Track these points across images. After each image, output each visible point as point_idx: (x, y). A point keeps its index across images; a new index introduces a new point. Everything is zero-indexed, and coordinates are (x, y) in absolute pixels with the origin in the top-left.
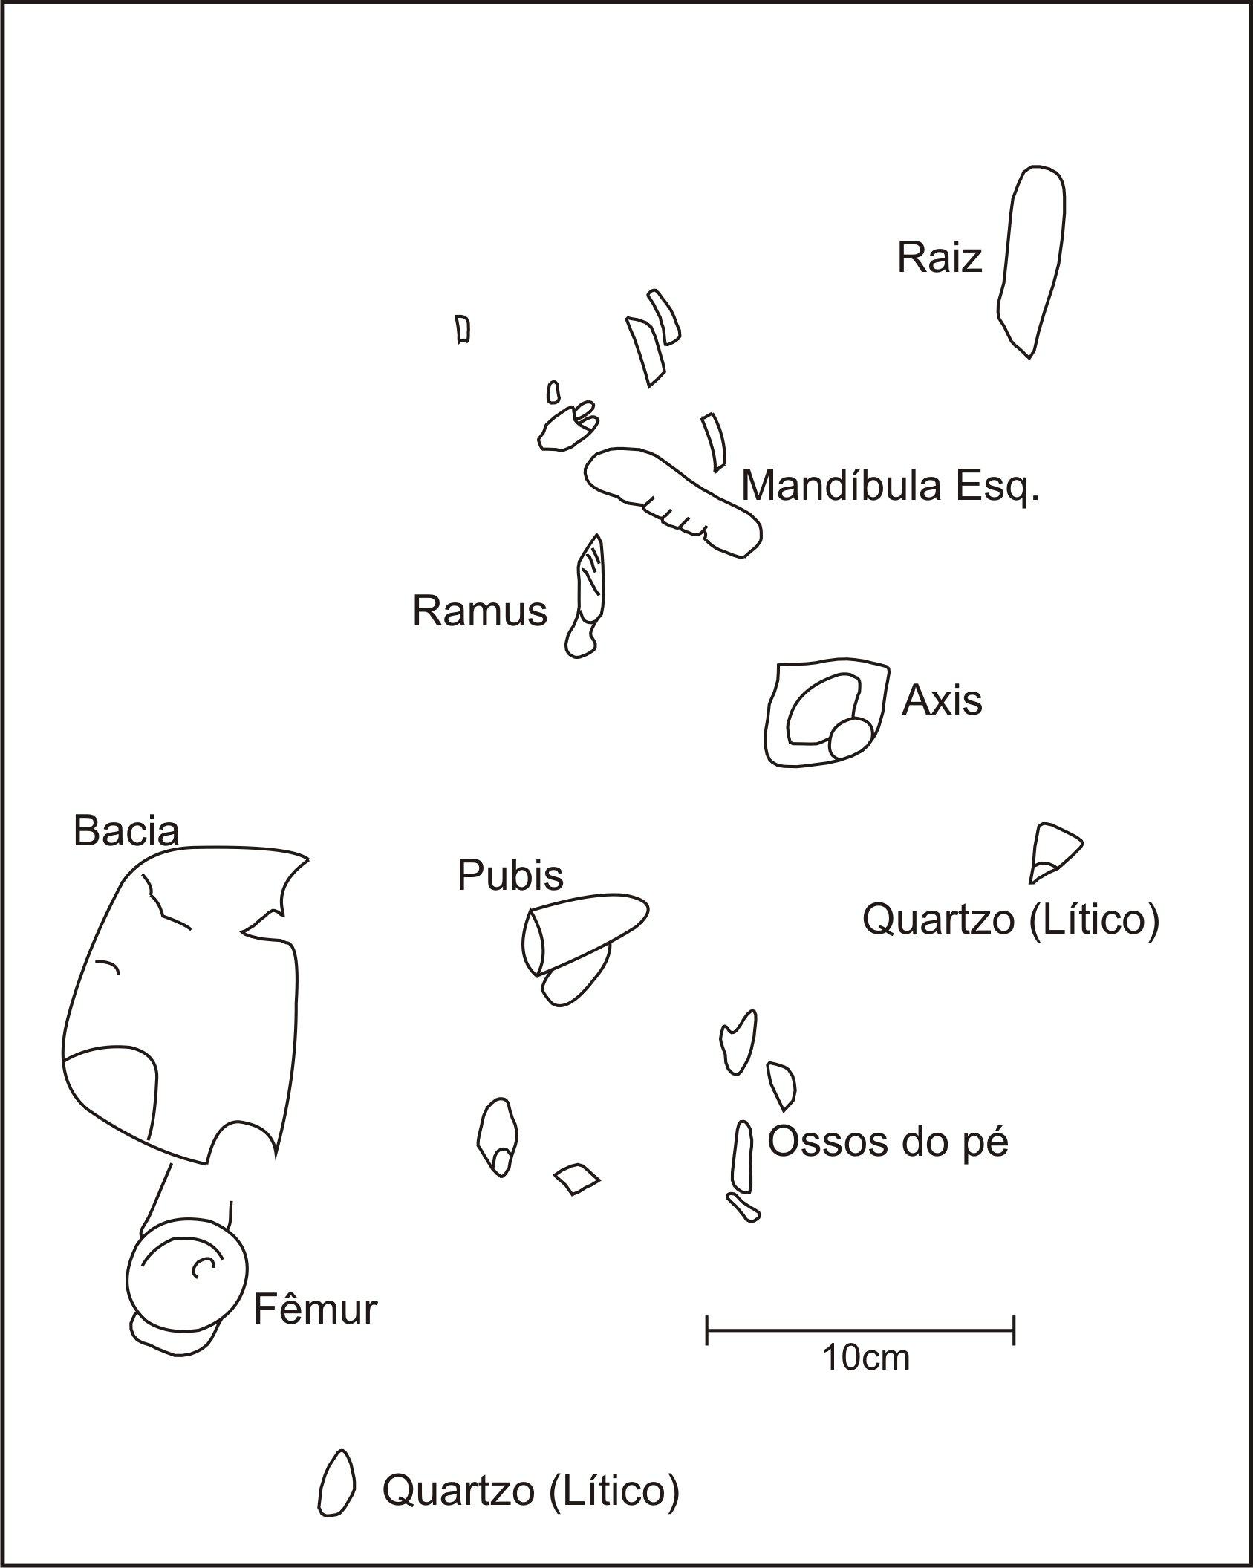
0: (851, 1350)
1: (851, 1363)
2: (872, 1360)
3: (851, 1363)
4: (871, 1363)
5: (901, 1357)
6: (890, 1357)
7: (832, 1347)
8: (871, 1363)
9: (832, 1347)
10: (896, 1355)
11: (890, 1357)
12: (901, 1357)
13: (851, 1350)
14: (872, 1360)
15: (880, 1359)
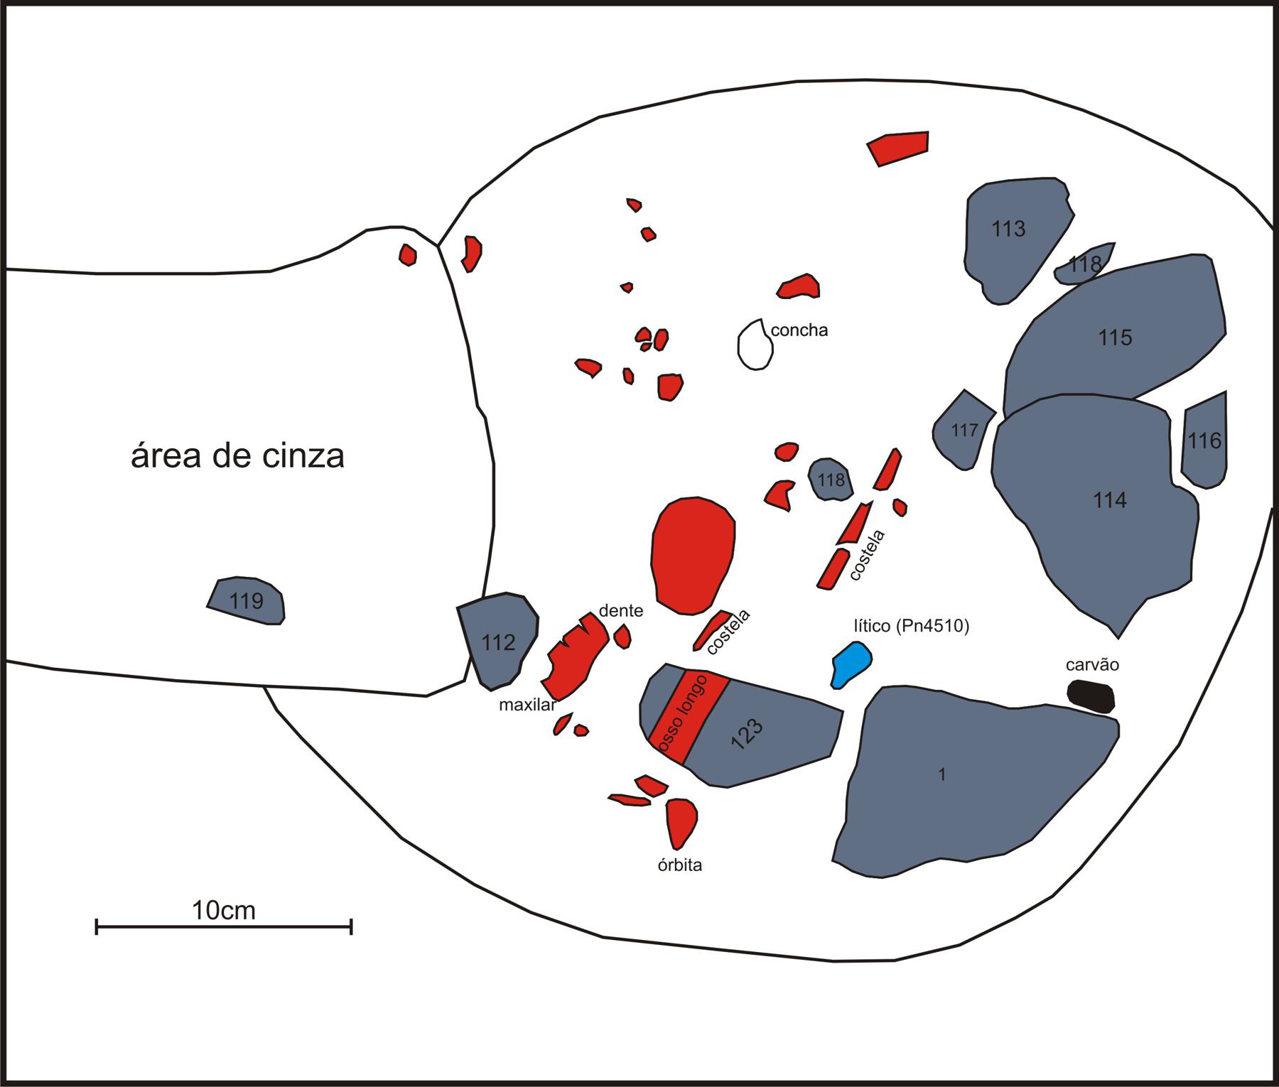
0: (213, 906)
1: (213, 914)
2: (228, 912)
3: (213, 914)
4: (227, 915)
5: (249, 910)
6: (241, 910)
7: (199, 903)
8: (227, 915)
9: (199, 903)
10: (245, 909)
11: (241, 910)
12: (249, 910)
13: (213, 906)
14: (228, 912)
15: (234, 912)
